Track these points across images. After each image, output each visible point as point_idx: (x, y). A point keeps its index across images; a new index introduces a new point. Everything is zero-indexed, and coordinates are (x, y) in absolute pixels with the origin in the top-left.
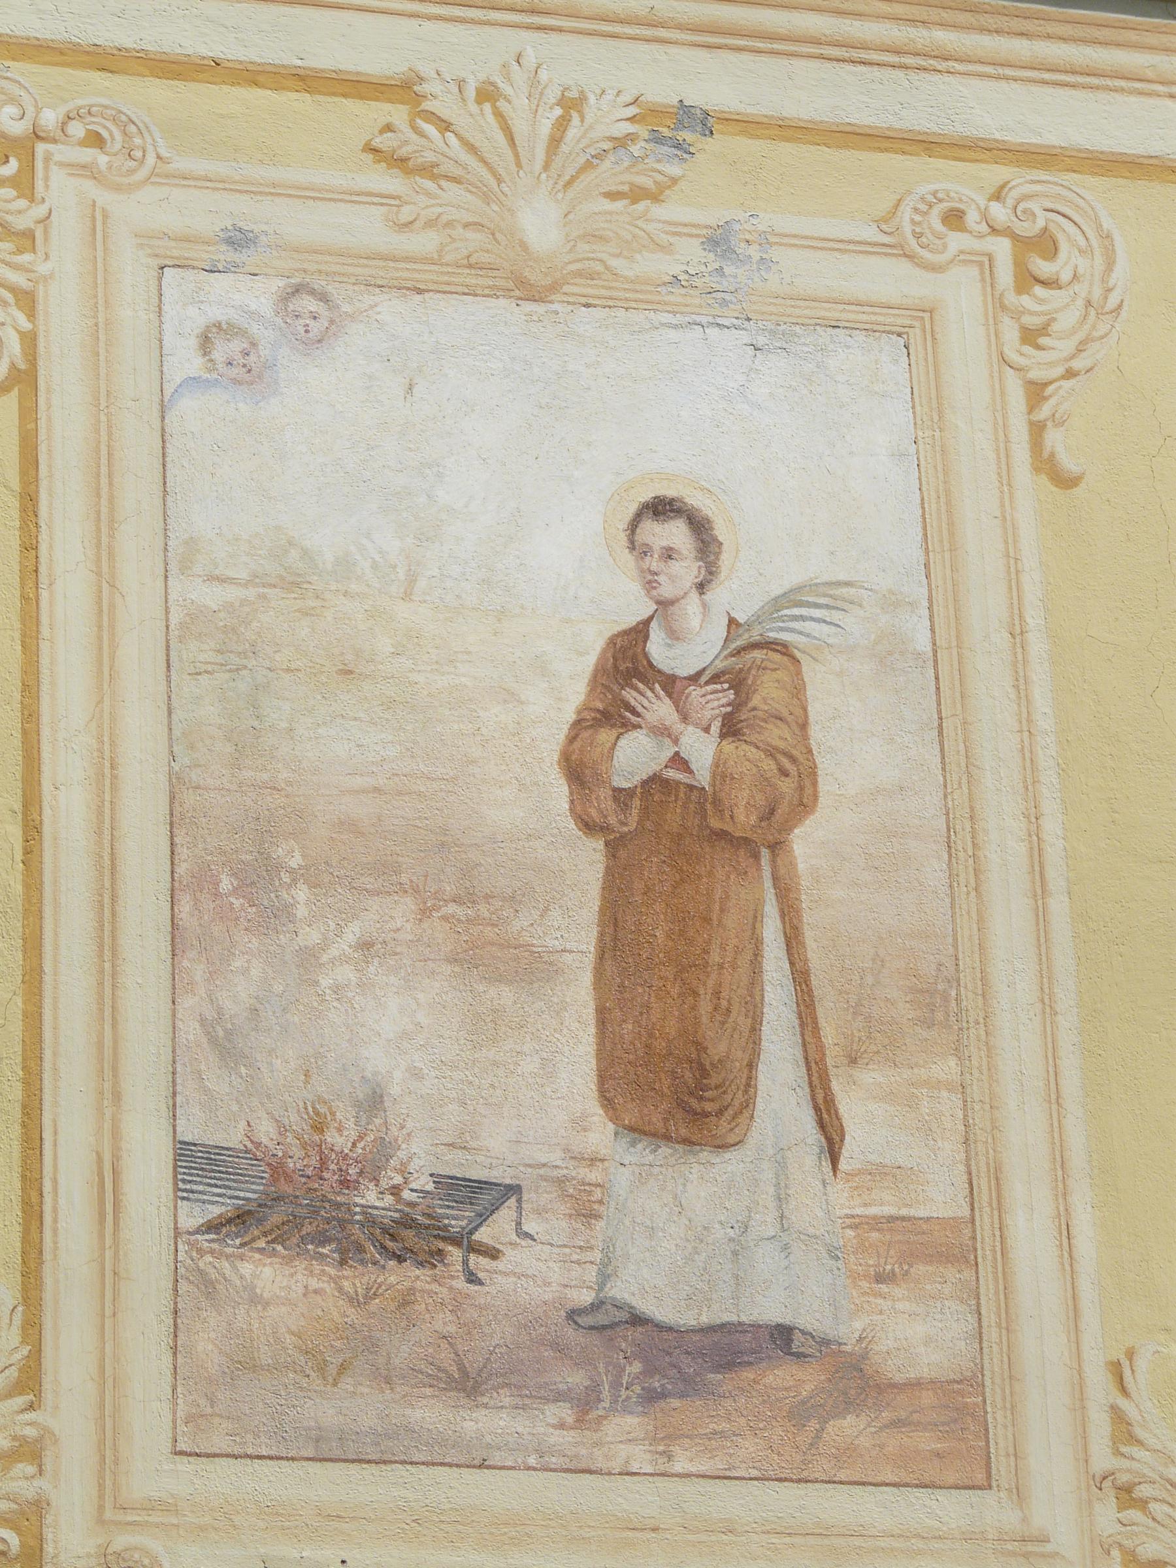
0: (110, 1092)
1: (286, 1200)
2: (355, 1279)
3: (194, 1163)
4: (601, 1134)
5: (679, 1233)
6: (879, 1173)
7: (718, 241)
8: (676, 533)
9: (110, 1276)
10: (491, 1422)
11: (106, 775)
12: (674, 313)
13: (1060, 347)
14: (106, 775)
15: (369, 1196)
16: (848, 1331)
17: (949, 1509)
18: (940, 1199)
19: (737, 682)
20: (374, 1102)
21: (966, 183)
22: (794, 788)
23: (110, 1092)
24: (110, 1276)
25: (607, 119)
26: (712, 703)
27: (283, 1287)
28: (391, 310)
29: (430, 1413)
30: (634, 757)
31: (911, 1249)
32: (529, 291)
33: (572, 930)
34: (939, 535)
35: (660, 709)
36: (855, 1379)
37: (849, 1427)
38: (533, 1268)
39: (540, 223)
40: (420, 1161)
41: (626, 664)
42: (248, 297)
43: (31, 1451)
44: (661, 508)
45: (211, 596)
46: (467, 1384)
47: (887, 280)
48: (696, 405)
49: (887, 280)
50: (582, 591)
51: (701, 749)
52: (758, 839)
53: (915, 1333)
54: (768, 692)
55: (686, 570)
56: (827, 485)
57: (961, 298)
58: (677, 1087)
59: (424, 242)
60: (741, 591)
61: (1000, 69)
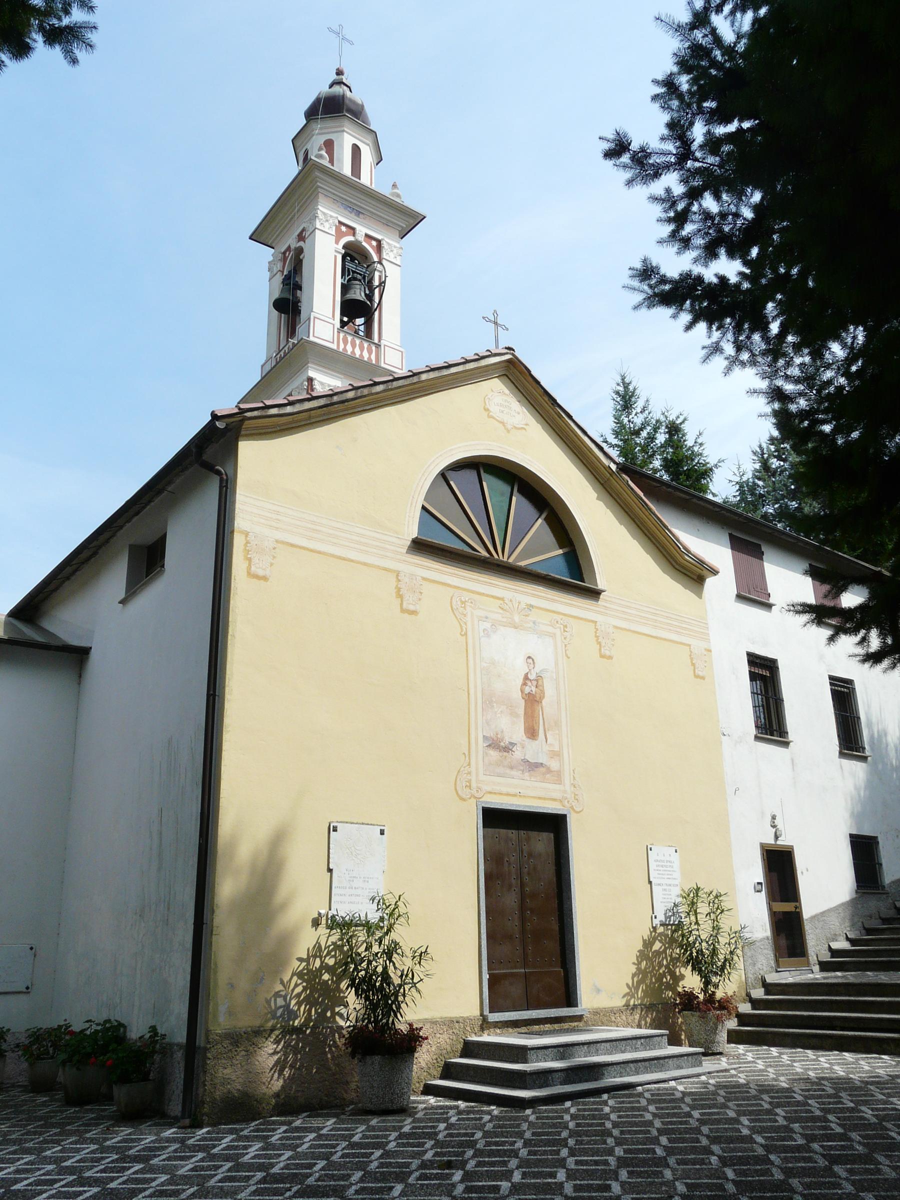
0: (476, 729)
1: (495, 744)
2: (501, 754)
3: (485, 738)
4: (524, 738)
5: (533, 750)
6: (551, 745)
7: (534, 623)
8: (530, 661)
9: (477, 752)
10: (514, 773)
11: (476, 687)
12: (678, 633)
13: (568, 639)
14: (476, 687)
15: (502, 744)
16: (548, 764)
17: (557, 787)
18: (557, 749)
19: (537, 681)
20: (502, 732)
21: (556, 616)
22: (542, 697)
23: (476, 729)
24: (477, 752)
25: (523, 605)
26: (535, 683)
27: (494, 754)
28: (502, 628)
29: (508, 771)
30: (527, 690)
31: (556, 755)
32: (516, 628)
33: (521, 712)
34: (556, 664)
35: (529, 684)
36: (549, 771)
37: (548, 776)
38: (518, 754)
39: (517, 618)
40: (507, 740)
41: (526, 678)
42: (487, 625)
43: (469, 773)
44: (529, 657)
45: (485, 665)
46: (512, 768)
47: (550, 629)
48: (533, 644)
49: (550, 629)
50: (521, 668)
51: (534, 689)
52: (539, 702)
53: (554, 765)
54: (540, 682)
55: (532, 666)
56: (546, 655)
57: (558, 632)
58: (532, 733)
59: (505, 620)
60: (537, 669)
61: (562, 603)
